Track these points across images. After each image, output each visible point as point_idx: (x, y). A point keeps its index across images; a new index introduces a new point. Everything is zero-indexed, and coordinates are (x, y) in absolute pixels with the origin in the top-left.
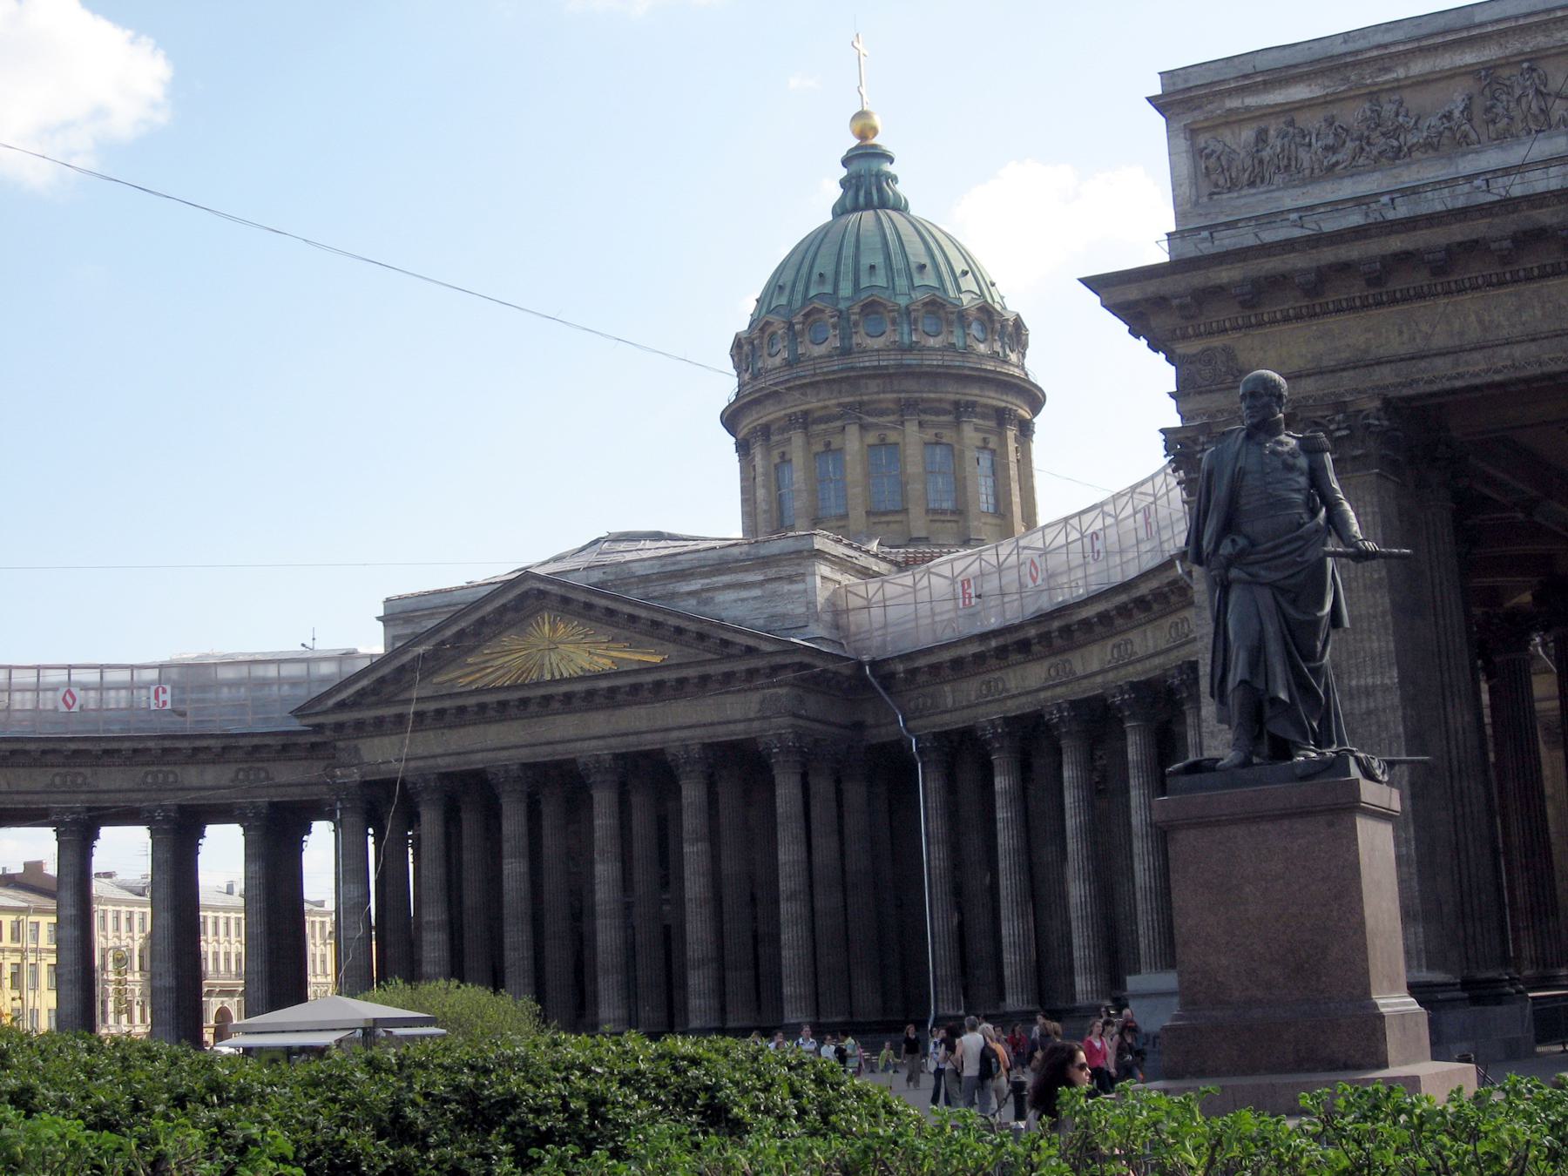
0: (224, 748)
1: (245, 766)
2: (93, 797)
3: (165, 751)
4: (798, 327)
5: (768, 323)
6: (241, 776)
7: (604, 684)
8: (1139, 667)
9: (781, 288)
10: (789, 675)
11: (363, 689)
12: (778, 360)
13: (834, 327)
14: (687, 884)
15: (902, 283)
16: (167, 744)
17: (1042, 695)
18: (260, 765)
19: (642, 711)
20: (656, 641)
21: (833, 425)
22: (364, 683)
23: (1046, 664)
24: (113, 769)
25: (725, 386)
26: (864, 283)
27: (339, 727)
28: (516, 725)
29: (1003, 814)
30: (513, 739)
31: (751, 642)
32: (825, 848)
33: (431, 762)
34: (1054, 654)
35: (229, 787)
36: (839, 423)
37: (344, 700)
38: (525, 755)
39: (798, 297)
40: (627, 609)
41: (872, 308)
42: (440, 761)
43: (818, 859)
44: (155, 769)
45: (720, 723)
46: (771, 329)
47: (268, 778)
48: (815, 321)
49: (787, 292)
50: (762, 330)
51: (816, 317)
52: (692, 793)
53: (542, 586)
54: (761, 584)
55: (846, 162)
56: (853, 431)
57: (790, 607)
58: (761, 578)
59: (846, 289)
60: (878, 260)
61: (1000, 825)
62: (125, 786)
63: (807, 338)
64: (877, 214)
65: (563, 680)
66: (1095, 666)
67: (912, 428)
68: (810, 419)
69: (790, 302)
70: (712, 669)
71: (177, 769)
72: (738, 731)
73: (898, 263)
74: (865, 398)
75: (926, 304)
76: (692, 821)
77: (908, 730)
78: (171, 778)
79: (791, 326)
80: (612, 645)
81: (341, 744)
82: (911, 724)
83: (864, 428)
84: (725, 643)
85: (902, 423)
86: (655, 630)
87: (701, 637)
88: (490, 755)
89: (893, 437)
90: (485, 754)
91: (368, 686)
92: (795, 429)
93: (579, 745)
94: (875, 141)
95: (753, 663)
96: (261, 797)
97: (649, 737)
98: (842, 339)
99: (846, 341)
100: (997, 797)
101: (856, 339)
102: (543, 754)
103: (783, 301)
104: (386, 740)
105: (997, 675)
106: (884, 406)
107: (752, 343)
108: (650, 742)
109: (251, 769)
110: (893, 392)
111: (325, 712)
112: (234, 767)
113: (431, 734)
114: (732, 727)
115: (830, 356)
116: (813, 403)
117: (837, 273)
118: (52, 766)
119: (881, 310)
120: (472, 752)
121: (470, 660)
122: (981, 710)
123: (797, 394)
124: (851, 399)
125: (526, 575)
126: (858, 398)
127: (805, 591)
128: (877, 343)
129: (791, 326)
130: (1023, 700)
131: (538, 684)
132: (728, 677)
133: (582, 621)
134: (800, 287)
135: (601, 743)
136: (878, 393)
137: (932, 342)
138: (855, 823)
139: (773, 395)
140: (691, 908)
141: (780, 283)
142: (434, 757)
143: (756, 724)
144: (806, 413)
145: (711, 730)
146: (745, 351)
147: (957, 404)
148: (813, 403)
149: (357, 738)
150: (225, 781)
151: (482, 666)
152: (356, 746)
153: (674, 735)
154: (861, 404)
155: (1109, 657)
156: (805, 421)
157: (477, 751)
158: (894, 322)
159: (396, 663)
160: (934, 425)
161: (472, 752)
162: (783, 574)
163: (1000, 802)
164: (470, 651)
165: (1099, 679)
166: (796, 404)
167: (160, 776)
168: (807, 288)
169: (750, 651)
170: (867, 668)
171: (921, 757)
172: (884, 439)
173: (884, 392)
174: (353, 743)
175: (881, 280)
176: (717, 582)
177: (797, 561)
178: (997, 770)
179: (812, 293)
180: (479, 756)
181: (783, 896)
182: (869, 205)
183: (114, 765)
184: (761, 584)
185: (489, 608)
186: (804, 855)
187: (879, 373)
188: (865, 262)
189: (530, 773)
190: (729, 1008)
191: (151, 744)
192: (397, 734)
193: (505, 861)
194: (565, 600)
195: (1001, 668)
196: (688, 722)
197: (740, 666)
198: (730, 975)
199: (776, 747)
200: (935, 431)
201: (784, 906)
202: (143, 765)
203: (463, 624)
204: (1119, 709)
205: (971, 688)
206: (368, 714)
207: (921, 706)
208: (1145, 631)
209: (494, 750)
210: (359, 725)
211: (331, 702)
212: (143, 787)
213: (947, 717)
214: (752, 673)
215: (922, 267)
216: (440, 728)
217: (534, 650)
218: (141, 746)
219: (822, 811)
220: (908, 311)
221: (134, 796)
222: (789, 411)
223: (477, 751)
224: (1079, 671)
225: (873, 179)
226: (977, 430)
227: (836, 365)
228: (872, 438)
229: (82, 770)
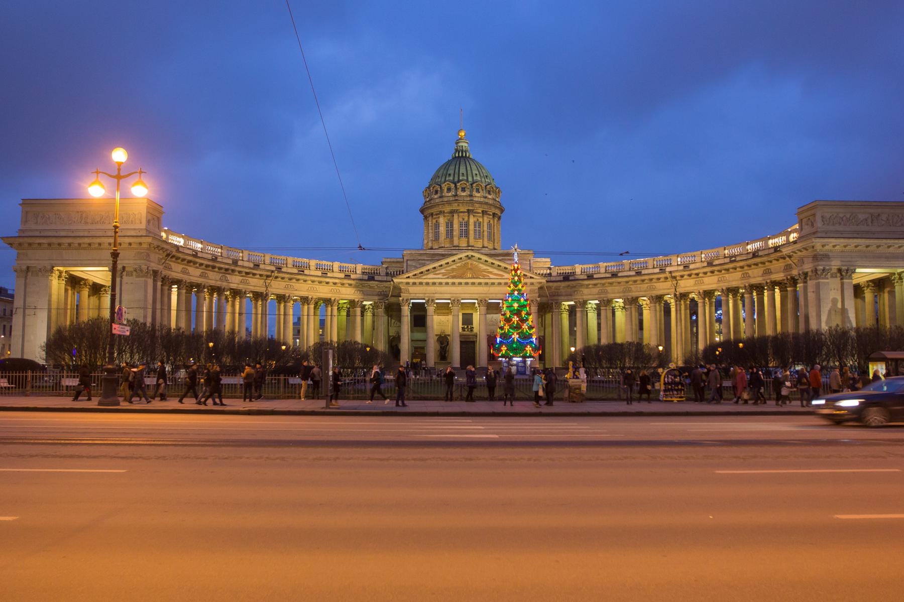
6: (356, 292)
15: (483, 180)
26: (475, 178)
49: (452, 175)
59: (470, 179)
60: (477, 173)
67: (485, 218)
69: (454, 179)
73: (482, 175)
83: (474, 216)
101: (474, 193)
103: (451, 178)
111: (404, 278)
124: (471, 208)
134: (456, 176)
137: (490, 197)
141: (448, 173)
179: (461, 178)
187: (480, 203)
206: (417, 281)
215: (487, 176)
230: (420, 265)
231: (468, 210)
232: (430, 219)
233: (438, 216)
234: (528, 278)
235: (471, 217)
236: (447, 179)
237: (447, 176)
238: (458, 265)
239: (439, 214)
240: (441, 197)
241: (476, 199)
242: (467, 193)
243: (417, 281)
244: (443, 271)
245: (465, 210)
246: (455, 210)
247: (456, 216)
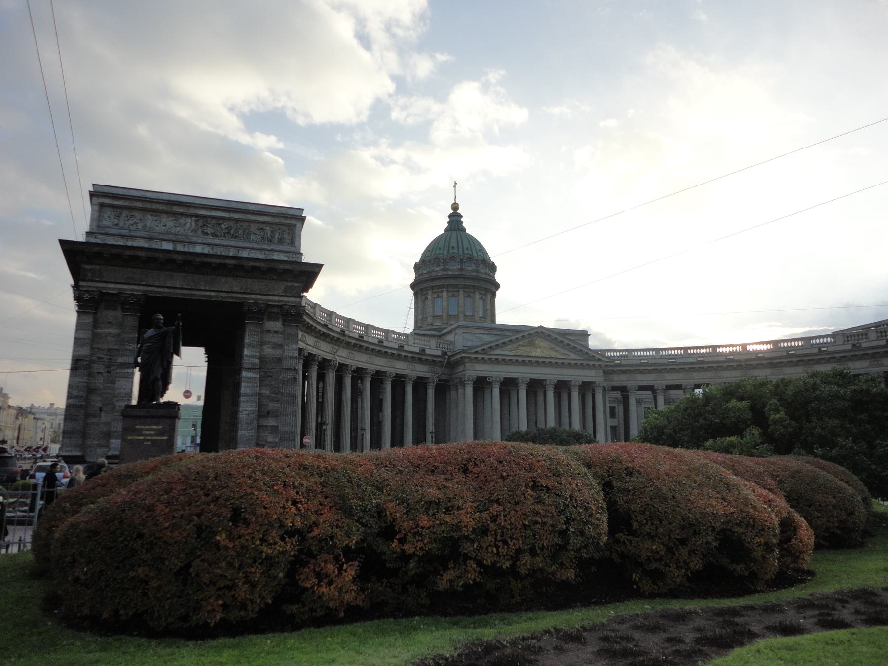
5: (453, 257)
9: (453, 247)
12: (455, 268)
13: (474, 264)
49: (456, 249)
55: (449, 216)
59: (475, 255)
65: (542, 357)
79: (461, 260)
83: (480, 293)
84: (593, 356)
86: (573, 349)
88: (520, 375)
89: (484, 297)
94: (458, 211)
95: (600, 363)
103: (455, 251)
111: (471, 353)
115: (472, 271)
116: (468, 283)
117: (471, 248)
122: (628, 382)
125: (541, 327)
128: (483, 271)
131: (533, 357)
134: (461, 249)
139: (455, 277)
141: (452, 245)
144: (465, 285)
148: (468, 283)
156: (465, 287)
158: (486, 267)
160: (436, 292)
166: (461, 282)
168: (463, 250)
169: (599, 360)
179: (466, 252)
182: (454, 230)
197: (597, 363)
205: (624, 377)
211: (473, 351)
213: (616, 383)
227: (474, 274)
230: (476, 339)
231: (473, 286)
232: (430, 292)
233: (439, 290)
234: (595, 360)
236: (451, 251)
237: (451, 249)
238: (525, 341)
239: (442, 288)
240: (444, 270)
241: (480, 275)
242: (473, 267)
243: (486, 357)
244: (510, 347)
247: (461, 292)
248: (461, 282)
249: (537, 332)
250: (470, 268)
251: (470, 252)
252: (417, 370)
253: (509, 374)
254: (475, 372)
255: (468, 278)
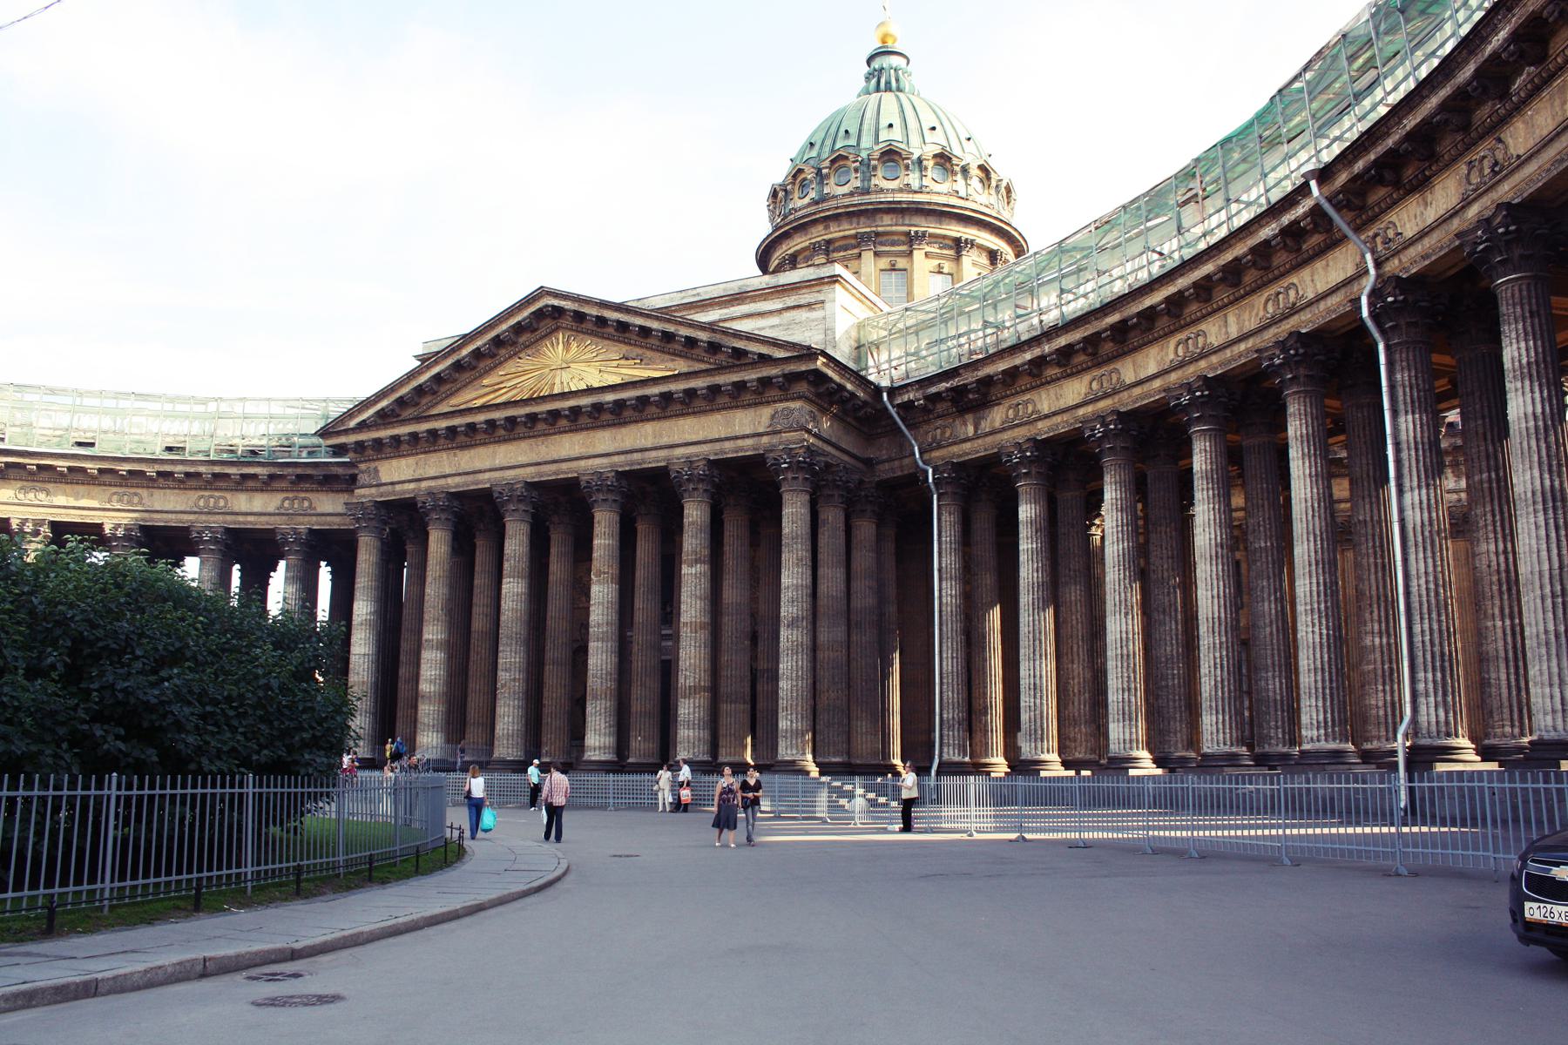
0: (272, 477)
1: (291, 495)
2: (146, 515)
3: (216, 476)
4: (824, 171)
6: (286, 504)
7: (610, 397)
8: (1214, 359)
10: (803, 388)
11: (383, 409)
12: (807, 200)
13: (856, 170)
14: (683, 607)
15: (915, 139)
16: (217, 469)
17: (1081, 412)
18: (303, 495)
19: (649, 428)
20: (667, 357)
21: (850, 252)
22: (384, 403)
23: (1087, 378)
24: (168, 491)
25: (761, 227)
27: (360, 446)
28: (524, 445)
29: (1027, 545)
30: (522, 459)
31: (764, 350)
32: (831, 580)
33: (442, 482)
34: (1098, 365)
35: (274, 514)
36: (856, 251)
37: (364, 421)
38: (529, 474)
39: (827, 149)
40: (639, 321)
41: (891, 155)
42: (450, 481)
43: (823, 588)
44: (207, 493)
45: (727, 439)
46: (803, 176)
47: (310, 506)
48: (841, 167)
50: (795, 177)
51: (841, 163)
52: (695, 513)
53: (556, 302)
54: (780, 311)
56: (868, 256)
57: (806, 334)
58: (780, 306)
59: (867, 142)
60: (897, 123)
61: (1023, 558)
62: (178, 508)
63: (832, 181)
64: (898, 97)
66: (1152, 369)
67: (918, 255)
68: (831, 248)
69: (819, 155)
70: (723, 379)
71: (228, 495)
72: (747, 447)
74: (880, 229)
75: (935, 156)
76: (693, 541)
77: (924, 463)
78: (222, 503)
80: (623, 362)
81: (363, 466)
82: (926, 456)
83: (876, 254)
84: (739, 354)
85: (911, 252)
87: (714, 348)
90: (492, 473)
91: (387, 406)
92: (818, 255)
93: (583, 463)
96: (303, 524)
97: (654, 454)
98: (863, 181)
99: (866, 183)
100: (1021, 526)
101: (874, 181)
102: (548, 473)
104: (403, 461)
105: (1027, 397)
106: (896, 238)
107: (786, 191)
108: (654, 459)
109: (296, 498)
110: (903, 225)
111: (347, 432)
112: (281, 496)
113: (444, 455)
114: (740, 443)
115: (851, 194)
116: (836, 232)
118: (110, 485)
119: (897, 158)
120: (480, 472)
121: (485, 382)
123: (821, 227)
124: (868, 230)
125: (542, 292)
126: (874, 229)
127: (824, 318)
129: (819, 170)
130: (1058, 419)
132: (740, 386)
133: (595, 339)
134: (829, 142)
135: (605, 461)
136: (891, 225)
138: (864, 559)
140: (685, 633)
142: (445, 477)
143: (765, 440)
144: (829, 242)
145: (717, 446)
146: (778, 196)
147: (957, 241)
149: (378, 459)
150: (271, 509)
151: (496, 387)
152: (376, 471)
153: (679, 452)
154: (877, 234)
155: (1172, 356)
157: (485, 471)
158: (907, 167)
159: (415, 384)
161: (480, 472)
162: (803, 302)
163: (1024, 532)
164: (487, 372)
165: (1157, 384)
167: (212, 500)
169: (764, 359)
170: (885, 395)
171: (937, 489)
172: (894, 265)
173: (896, 225)
174: (373, 465)
175: (896, 134)
176: (735, 312)
177: (817, 288)
178: (1022, 498)
179: (838, 146)
180: (487, 476)
181: (784, 623)
183: (169, 488)
184: (780, 311)
185: (504, 327)
186: (809, 581)
188: (884, 123)
189: (535, 494)
190: (722, 742)
191: (202, 469)
192: (413, 455)
193: (504, 581)
194: (580, 317)
195: (1033, 388)
196: (694, 438)
197: (751, 375)
198: (725, 707)
199: (785, 463)
200: (937, 262)
201: (784, 633)
202: (196, 489)
203: (479, 343)
204: (1185, 409)
206: (384, 434)
207: (938, 437)
208: (1225, 315)
209: (501, 469)
210: (378, 443)
211: (352, 424)
212: (196, 509)
213: (967, 446)
214: (765, 382)
216: (453, 448)
217: (547, 370)
218: (192, 470)
219: (831, 539)
220: (920, 161)
221: (186, 517)
222: (813, 241)
223: (485, 471)
224: (1129, 376)
225: (892, 71)
226: (974, 264)
227: (856, 200)
228: (884, 263)
229: (139, 491)
231: (855, 236)
235: (868, 256)
241: (882, 198)
243: (384, 434)
245: (853, 242)
246: (814, 244)
248: (818, 234)
249: (540, 314)
250: (839, 189)
251: (853, 142)
252: (319, 510)
253: (469, 478)
254: (373, 490)
255: (836, 218)
